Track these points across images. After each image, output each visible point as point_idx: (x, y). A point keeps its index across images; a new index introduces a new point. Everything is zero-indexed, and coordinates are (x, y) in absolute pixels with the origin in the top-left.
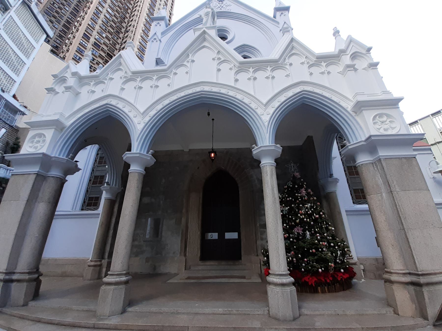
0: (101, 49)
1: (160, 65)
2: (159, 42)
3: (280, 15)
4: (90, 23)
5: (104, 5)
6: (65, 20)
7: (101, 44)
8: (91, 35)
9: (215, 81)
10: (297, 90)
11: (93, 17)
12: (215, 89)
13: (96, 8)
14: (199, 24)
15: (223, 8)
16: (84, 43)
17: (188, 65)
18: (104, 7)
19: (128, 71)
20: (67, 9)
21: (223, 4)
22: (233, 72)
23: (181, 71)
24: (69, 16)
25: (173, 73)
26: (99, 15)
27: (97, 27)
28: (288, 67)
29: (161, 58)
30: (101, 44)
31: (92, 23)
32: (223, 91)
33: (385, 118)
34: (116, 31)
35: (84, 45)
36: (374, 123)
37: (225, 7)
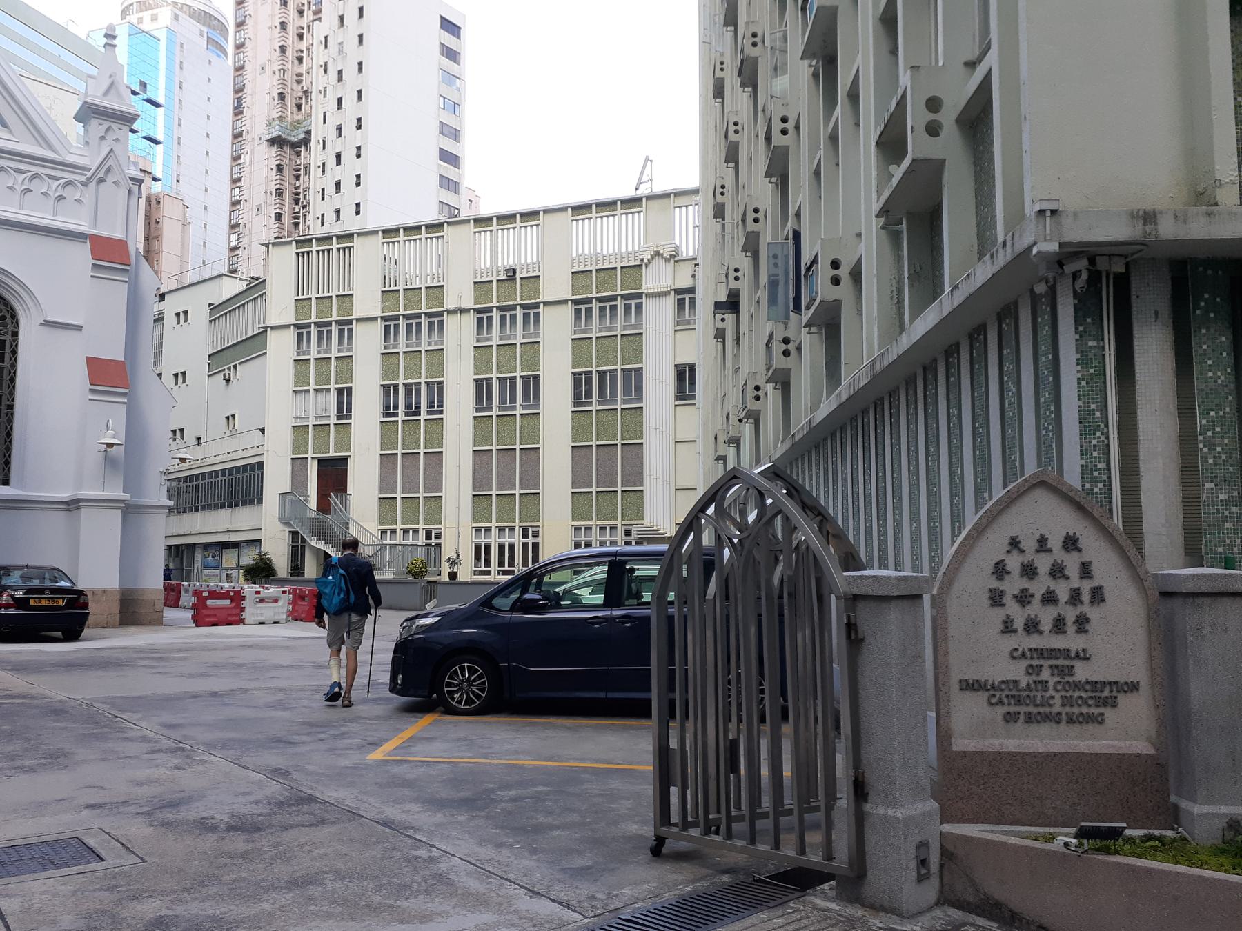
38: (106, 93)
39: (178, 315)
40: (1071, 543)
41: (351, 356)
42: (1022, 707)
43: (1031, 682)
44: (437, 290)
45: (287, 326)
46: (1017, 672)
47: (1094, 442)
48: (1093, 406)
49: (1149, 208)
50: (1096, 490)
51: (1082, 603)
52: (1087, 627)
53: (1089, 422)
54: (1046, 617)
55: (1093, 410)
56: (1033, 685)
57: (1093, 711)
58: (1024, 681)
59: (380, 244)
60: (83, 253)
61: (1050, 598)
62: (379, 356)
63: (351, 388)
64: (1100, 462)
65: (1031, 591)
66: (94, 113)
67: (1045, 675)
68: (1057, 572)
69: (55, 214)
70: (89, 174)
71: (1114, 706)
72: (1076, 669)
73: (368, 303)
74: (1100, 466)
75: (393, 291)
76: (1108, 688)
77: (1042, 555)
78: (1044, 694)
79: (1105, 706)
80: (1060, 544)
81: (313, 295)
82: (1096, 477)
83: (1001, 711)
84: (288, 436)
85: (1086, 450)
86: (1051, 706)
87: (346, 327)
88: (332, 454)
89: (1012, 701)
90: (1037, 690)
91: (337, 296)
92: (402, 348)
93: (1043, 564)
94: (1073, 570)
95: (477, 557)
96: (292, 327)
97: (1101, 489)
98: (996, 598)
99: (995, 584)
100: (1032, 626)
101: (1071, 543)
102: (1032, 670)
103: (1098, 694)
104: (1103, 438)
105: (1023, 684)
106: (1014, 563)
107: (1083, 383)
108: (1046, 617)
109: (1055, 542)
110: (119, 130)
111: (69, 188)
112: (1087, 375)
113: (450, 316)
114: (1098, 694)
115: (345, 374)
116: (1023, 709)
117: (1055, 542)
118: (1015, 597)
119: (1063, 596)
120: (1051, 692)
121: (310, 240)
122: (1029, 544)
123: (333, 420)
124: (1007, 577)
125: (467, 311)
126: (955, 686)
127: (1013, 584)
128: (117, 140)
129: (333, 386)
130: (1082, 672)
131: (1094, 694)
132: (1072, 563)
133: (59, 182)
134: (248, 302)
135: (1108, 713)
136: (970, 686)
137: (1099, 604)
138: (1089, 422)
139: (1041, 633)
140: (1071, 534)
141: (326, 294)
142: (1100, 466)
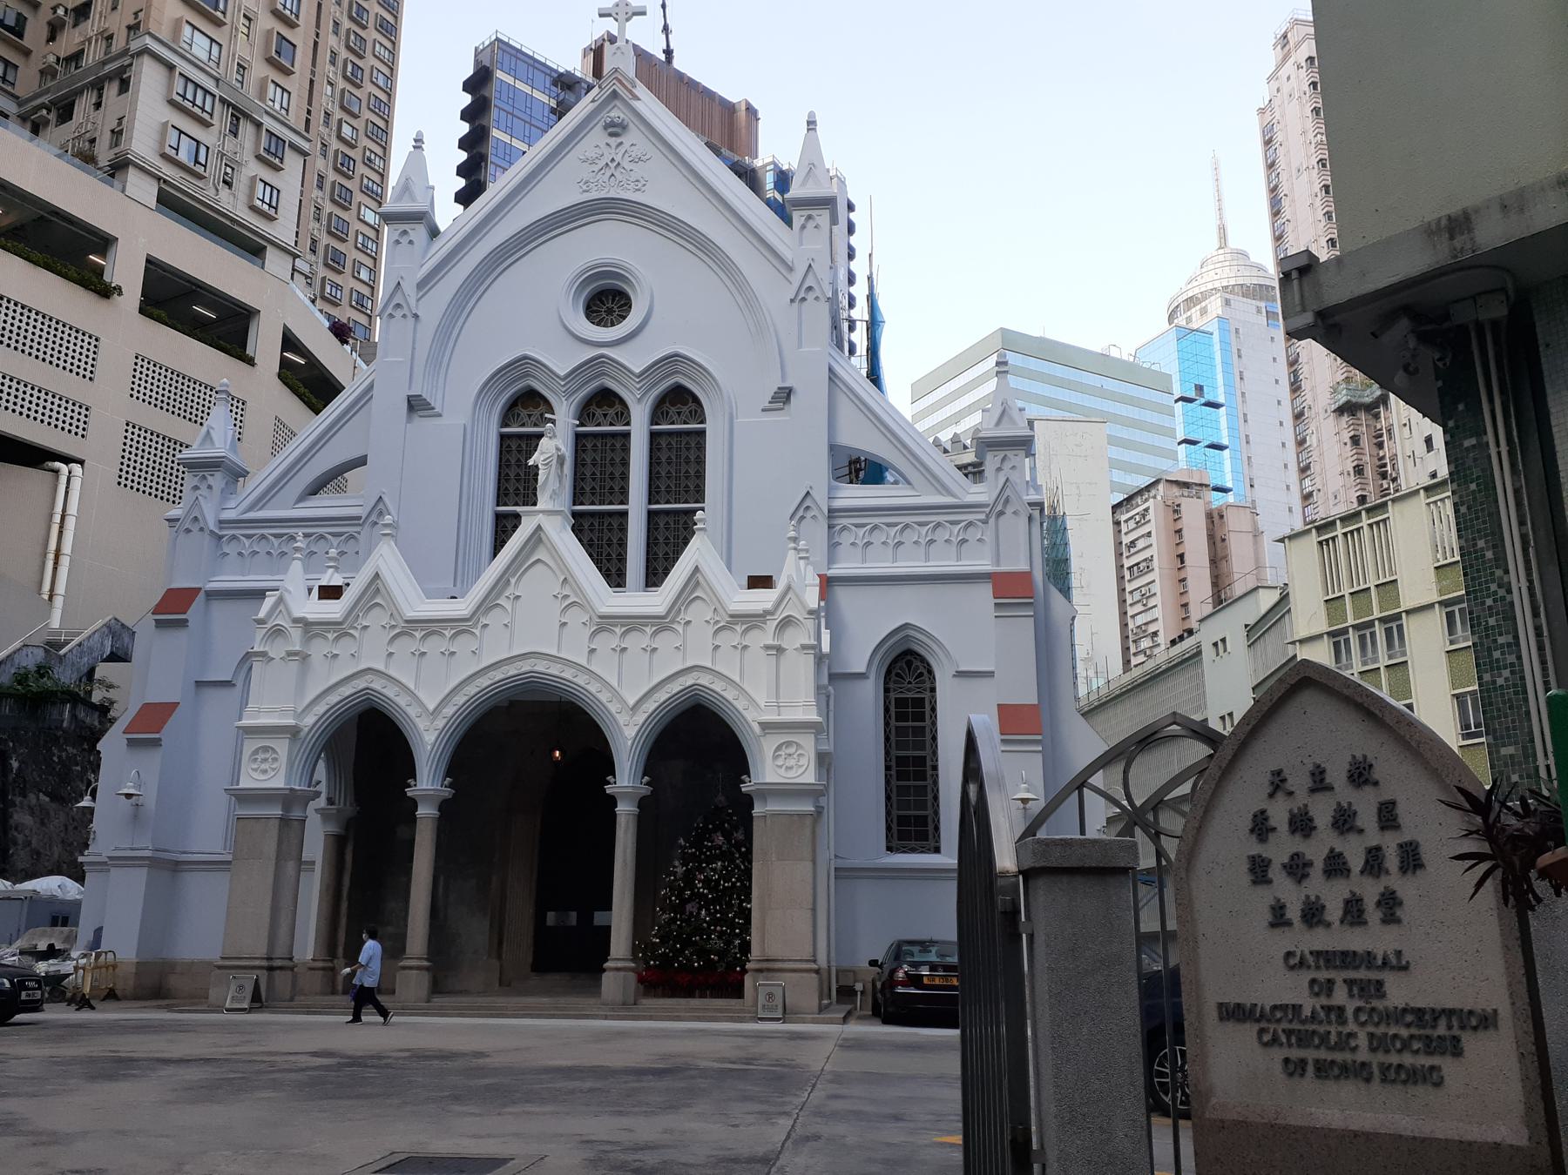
1: (421, 413)
2: (411, 320)
3: (803, 227)
9: (554, 652)
10: (688, 681)
12: (554, 670)
14: (541, 240)
15: (620, 169)
17: (507, 605)
19: (395, 612)
21: (622, 150)
22: (588, 631)
23: (490, 619)
25: (480, 625)
28: (680, 629)
29: (424, 396)
32: (568, 674)
33: (792, 750)
36: (775, 757)
37: (628, 166)
38: (998, 423)
39: (1215, 644)
40: (1360, 774)
41: (1406, 662)
42: (1309, 1051)
43: (1318, 1007)
45: (1319, 637)
46: (1293, 990)
47: (1489, 602)
48: (1481, 544)
49: (1454, 209)
50: (1500, 681)
51: (1387, 872)
52: (1399, 913)
53: (1478, 571)
54: (1333, 897)
55: (1482, 549)
56: (1322, 1014)
57: (1423, 1063)
58: (1309, 1004)
59: (1424, 505)
60: (985, 592)
61: (1336, 866)
62: (1444, 655)
64: (1501, 635)
65: (1308, 857)
66: (988, 446)
67: (1340, 996)
68: (1344, 821)
69: (864, 561)
70: (987, 510)
71: (1457, 1052)
72: (1388, 987)
74: (1501, 640)
75: (1450, 564)
76: (1443, 1022)
77: (1319, 796)
78: (1340, 1029)
79: (1443, 1054)
80: (1344, 775)
81: (1346, 591)
82: (1497, 660)
83: (1278, 1054)
85: (1478, 617)
86: (1354, 1049)
87: (1393, 625)
89: (1293, 1040)
90: (1329, 1023)
91: (1377, 586)
93: (1322, 812)
94: (1367, 817)
96: (1325, 636)
97: (1506, 679)
98: (1259, 870)
99: (1256, 849)
100: (1313, 914)
101: (1360, 774)
102: (1323, 988)
103: (1428, 1032)
104: (1502, 592)
105: (1307, 1012)
106: (1279, 813)
107: (1463, 509)
108: (1333, 897)
109: (1337, 775)
110: (1016, 457)
111: (970, 529)
112: (1468, 495)
114: (1428, 1032)
116: (1310, 1054)
117: (1337, 775)
118: (1284, 866)
119: (1356, 861)
120: (1352, 1026)
121: (1333, 523)
122: (1299, 781)
124: (1271, 836)
126: (1212, 1014)
127: (1280, 848)
128: (1013, 467)
130: (1399, 992)
131: (1422, 1032)
132: (1365, 806)
133: (960, 526)
134: (1283, 616)
135: (1447, 1064)
136: (1234, 1013)
137: (1414, 873)
138: (1478, 571)
139: (1328, 925)
140: (1359, 757)
142: (1501, 640)
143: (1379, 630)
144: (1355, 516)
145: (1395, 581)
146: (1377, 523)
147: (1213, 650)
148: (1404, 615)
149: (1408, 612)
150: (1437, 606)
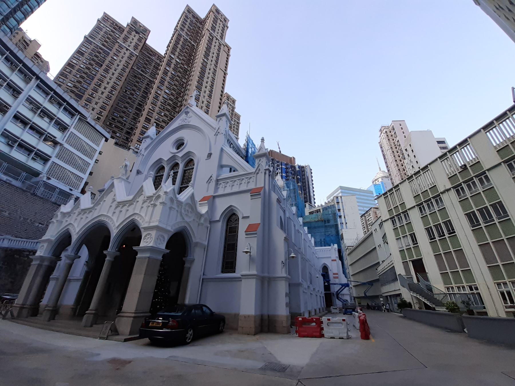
0: (160, 127)
4: (151, 107)
5: (162, 88)
6: (137, 103)
7: (160, 122)
8: (152, 117)
11: (153, 101)
13: (156, 92)
16: (146, 125)
18: (162, 90)
20: (138, 93)
24: (140, 99)
26: (158, 98)
27: (157, 109)
30: (160, 122)
31: (152, 107)
34: (173, 107)
35: (146, 127)
44: (434, 188)
63: (414, 233)
73: (410, 202)
84: (398, 254)
88: (415, 258)
92: (428, 213)
95: (504, 299)
113: (443, 195)
115: (411, 228)
123: (412, 246)
125: (450, 189)
129: (408, 234)
141: (396, 205)
143: (402, 215)
144: (392, 189)
145: (404, 202)
146: (397, 190)
147: (374, 231)
148: (408, 210)
149: (409, 209)
150: (416, 206)
